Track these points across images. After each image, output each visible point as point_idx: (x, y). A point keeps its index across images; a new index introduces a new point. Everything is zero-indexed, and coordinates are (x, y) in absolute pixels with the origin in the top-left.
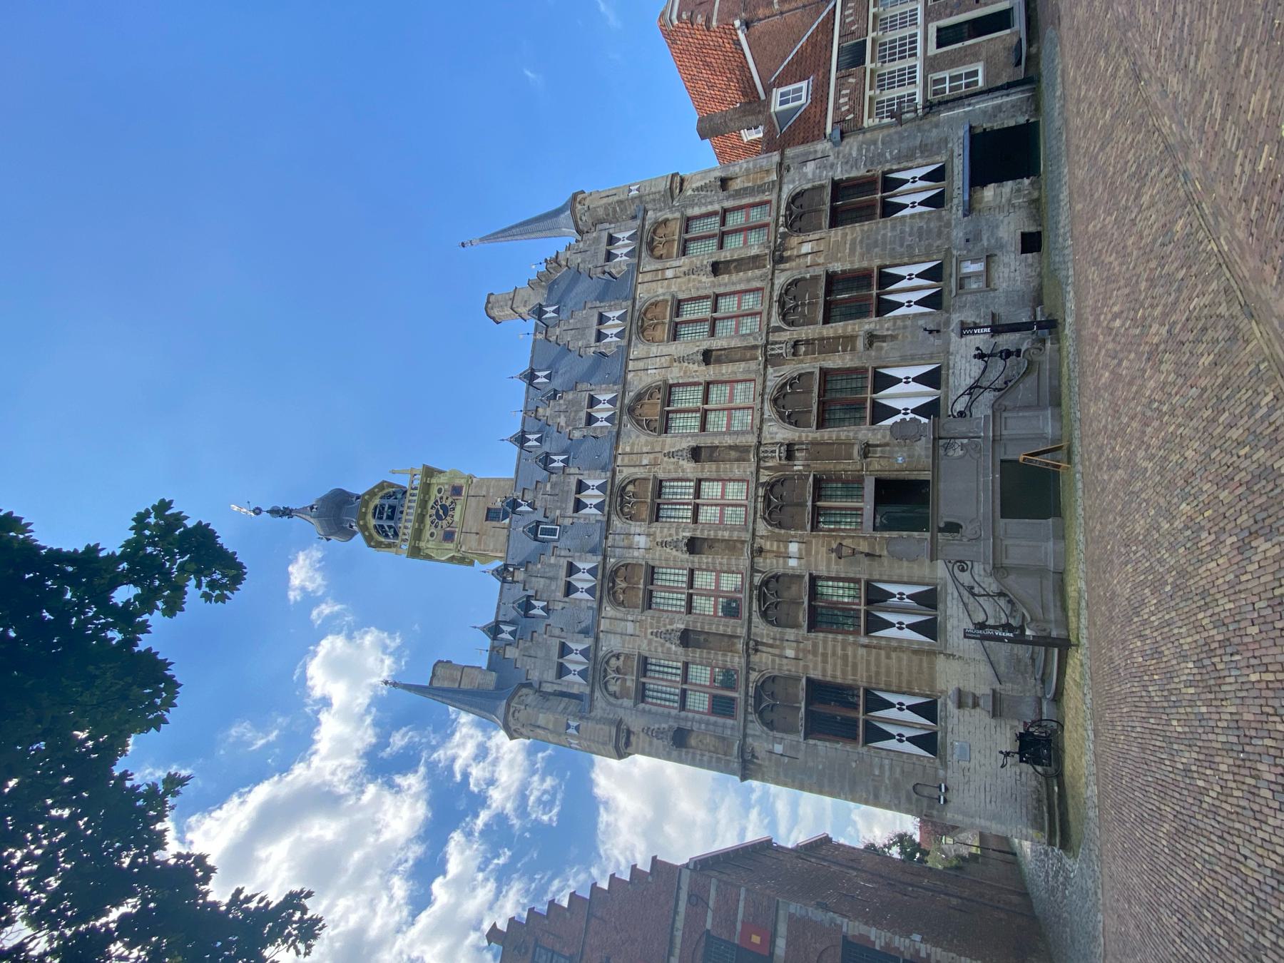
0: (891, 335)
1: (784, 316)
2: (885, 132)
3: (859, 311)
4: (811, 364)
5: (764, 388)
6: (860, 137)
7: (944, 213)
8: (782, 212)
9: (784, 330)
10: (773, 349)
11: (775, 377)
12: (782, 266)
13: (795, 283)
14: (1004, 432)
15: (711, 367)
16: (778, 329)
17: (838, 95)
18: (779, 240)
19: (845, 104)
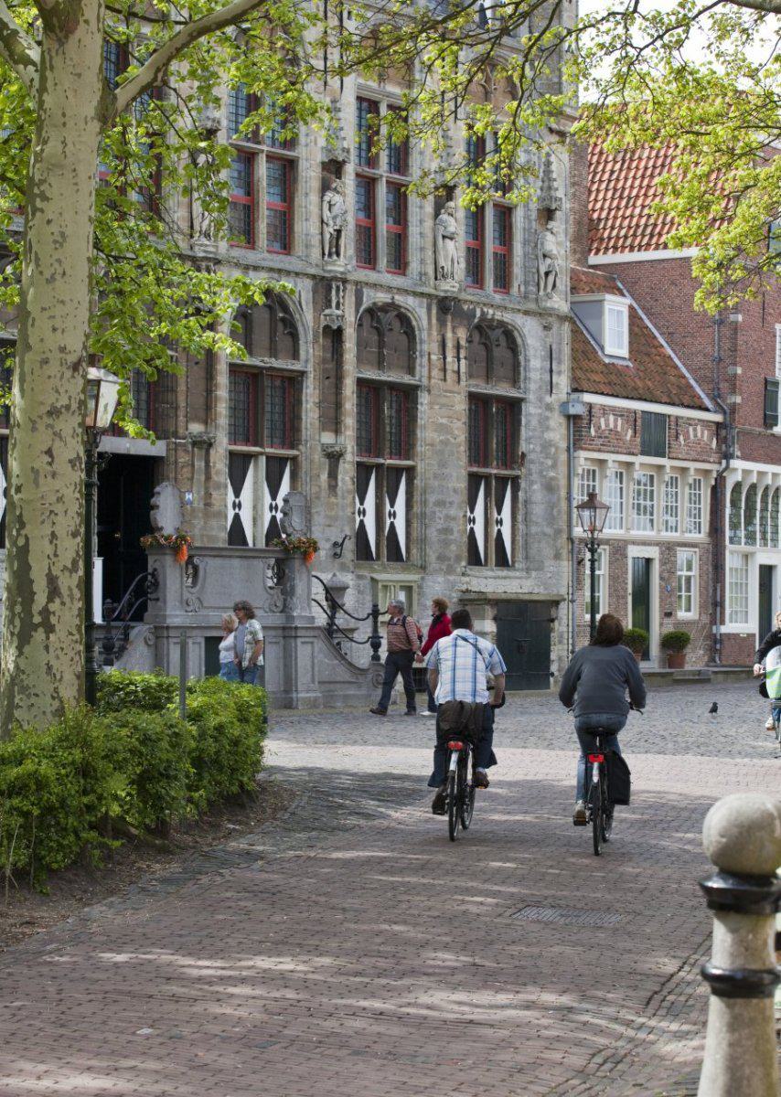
0: (336, 485)
1: (372, 312)
2: (563, 482)
3: (370, 440)
4: (310, 355)
5: (288, 273)
6: (563, 445)
7: (464, 563)
8: (498, 315)
9: (357, 311)
10: (338, 288)
11: (301, 291)
12: (434, 311)
13: (409, 332)
14: (299, 640)
15: (319, 169)
16: (359, 302)
17: (613, 410)
18: (465, 307)
19: (607, 425)
